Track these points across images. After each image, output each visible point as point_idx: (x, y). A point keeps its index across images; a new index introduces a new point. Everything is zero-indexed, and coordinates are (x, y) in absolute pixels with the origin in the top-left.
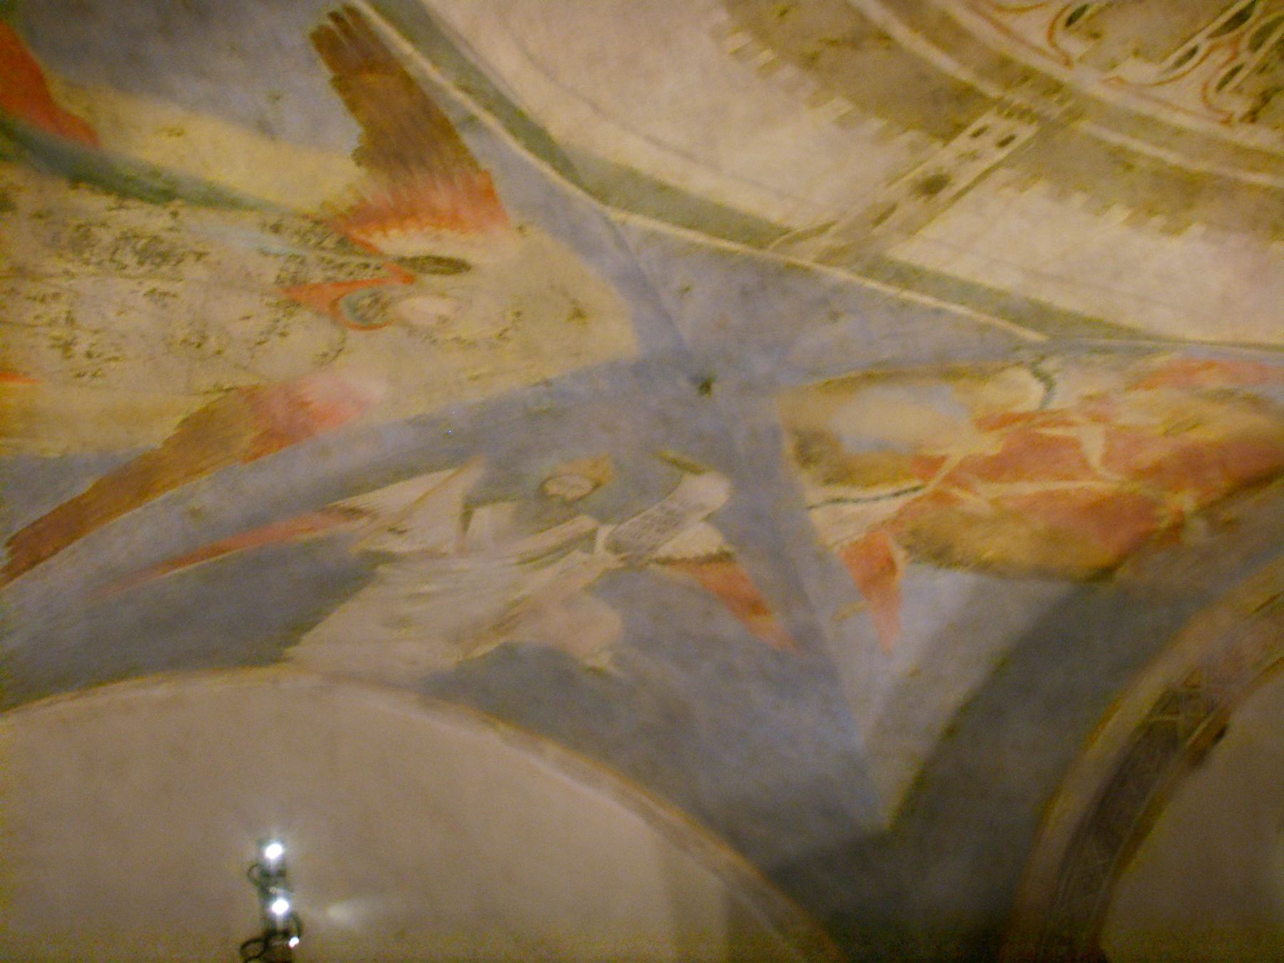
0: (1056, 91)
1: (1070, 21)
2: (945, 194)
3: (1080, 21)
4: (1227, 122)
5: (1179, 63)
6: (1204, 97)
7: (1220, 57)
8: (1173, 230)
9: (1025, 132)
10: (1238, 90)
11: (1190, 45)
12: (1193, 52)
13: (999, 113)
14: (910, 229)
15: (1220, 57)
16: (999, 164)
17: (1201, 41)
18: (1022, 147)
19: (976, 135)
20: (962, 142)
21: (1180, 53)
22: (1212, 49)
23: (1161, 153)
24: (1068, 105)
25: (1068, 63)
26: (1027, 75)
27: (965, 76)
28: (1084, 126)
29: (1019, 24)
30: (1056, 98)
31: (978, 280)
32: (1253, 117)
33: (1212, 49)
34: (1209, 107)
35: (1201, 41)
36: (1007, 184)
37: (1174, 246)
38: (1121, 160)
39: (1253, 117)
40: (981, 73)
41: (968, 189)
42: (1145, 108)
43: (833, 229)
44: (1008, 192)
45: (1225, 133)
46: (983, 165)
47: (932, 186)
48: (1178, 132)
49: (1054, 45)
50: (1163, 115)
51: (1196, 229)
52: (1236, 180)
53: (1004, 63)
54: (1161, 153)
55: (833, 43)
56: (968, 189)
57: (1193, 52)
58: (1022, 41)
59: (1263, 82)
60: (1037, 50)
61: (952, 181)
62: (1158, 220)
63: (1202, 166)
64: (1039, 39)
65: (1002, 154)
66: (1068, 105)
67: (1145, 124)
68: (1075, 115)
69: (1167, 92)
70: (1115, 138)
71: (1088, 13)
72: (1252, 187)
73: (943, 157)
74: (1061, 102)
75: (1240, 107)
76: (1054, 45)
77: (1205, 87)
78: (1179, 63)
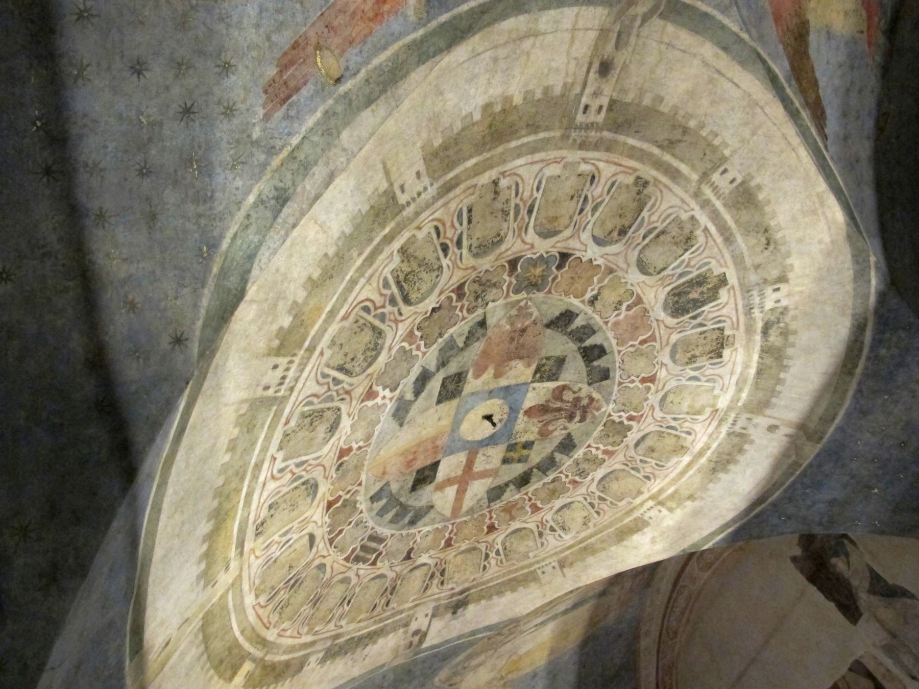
0: (580, 144)
1: (593, 177)
2: (596, 66)
3: (589, 178)
4: (503, 174)
5: (540, 182)
6: (519, 176)
7: (527, 194)
8: (487, 107)
9: (580, 118)
10: (509, 188)
11: (541, 191)
12: (538, 189)
13: (597, 124)
14: (603, 32)
15: (527, 194)
16: (582, 94)
17: (538, 195)
18: (577, 110)
19: (601, 107)
20: (605, 101)
21: (543, 186)
22: (532, 195)
23: (519, 142)
24: (570, 141)
25: (583, 159)
26: (596, 147)
27: (621, 138)
28: (557, 134)
29: (613, 169)
30: (578, 141)
31: (558, 11)
32: (495, 183)
33: (532, 195)
34: (515, 174)
35: (538, 195)
36: (573, 84)
37: (481, 100)
38: (534, 128)
39: (495, 183)
40: (616, 141)
41: (588, 72)
42: (538, 156)
43: (638, 23)
44: (570, 80)
45: (501, 169)
46: (588, 91)
47: (605, 68)
48: (519, 156)
49: (593, 164)
50: (529, 158)
51: (477, 117)
52: (481, 154)
53: (608, 149)
54: (519, 142)
55: (680, 141)
56: (588, 72)
57: (538, 189)
58: (607, 162)
59: (502, 198)
60: (599, 160)
61: (597, 75)
62: (498, 108)
63: (500, 149)
64: (601, 165)
65: (584, 100)
66: (570, 141)
67: (533, 149)
68: (565, 137)
69: (536, 168)
70: (542, 135)
71: (588, 183)
72: (471, 157)
73: (608, 90)
74: (575, 140)
75: (504, 183)
76: (593, 164)
77: (522, 180)
78: (540, 182)
